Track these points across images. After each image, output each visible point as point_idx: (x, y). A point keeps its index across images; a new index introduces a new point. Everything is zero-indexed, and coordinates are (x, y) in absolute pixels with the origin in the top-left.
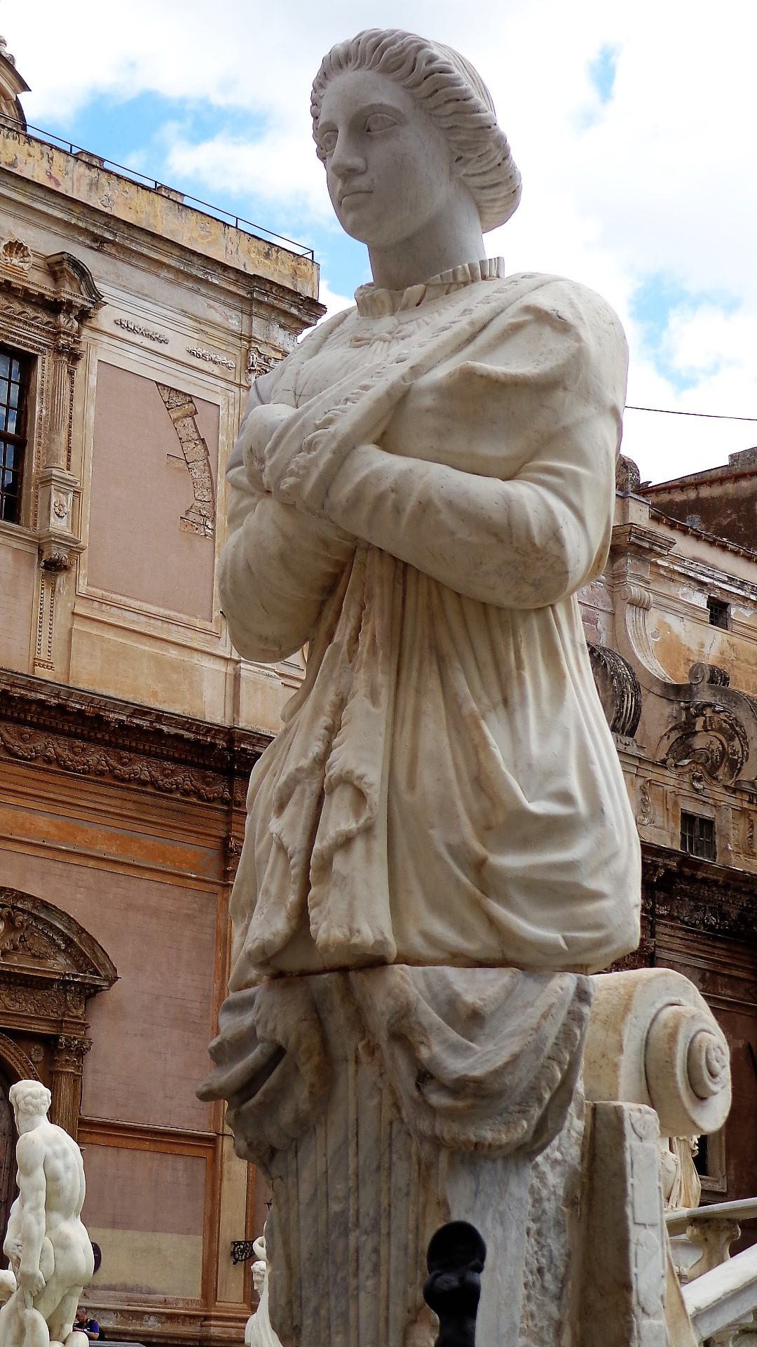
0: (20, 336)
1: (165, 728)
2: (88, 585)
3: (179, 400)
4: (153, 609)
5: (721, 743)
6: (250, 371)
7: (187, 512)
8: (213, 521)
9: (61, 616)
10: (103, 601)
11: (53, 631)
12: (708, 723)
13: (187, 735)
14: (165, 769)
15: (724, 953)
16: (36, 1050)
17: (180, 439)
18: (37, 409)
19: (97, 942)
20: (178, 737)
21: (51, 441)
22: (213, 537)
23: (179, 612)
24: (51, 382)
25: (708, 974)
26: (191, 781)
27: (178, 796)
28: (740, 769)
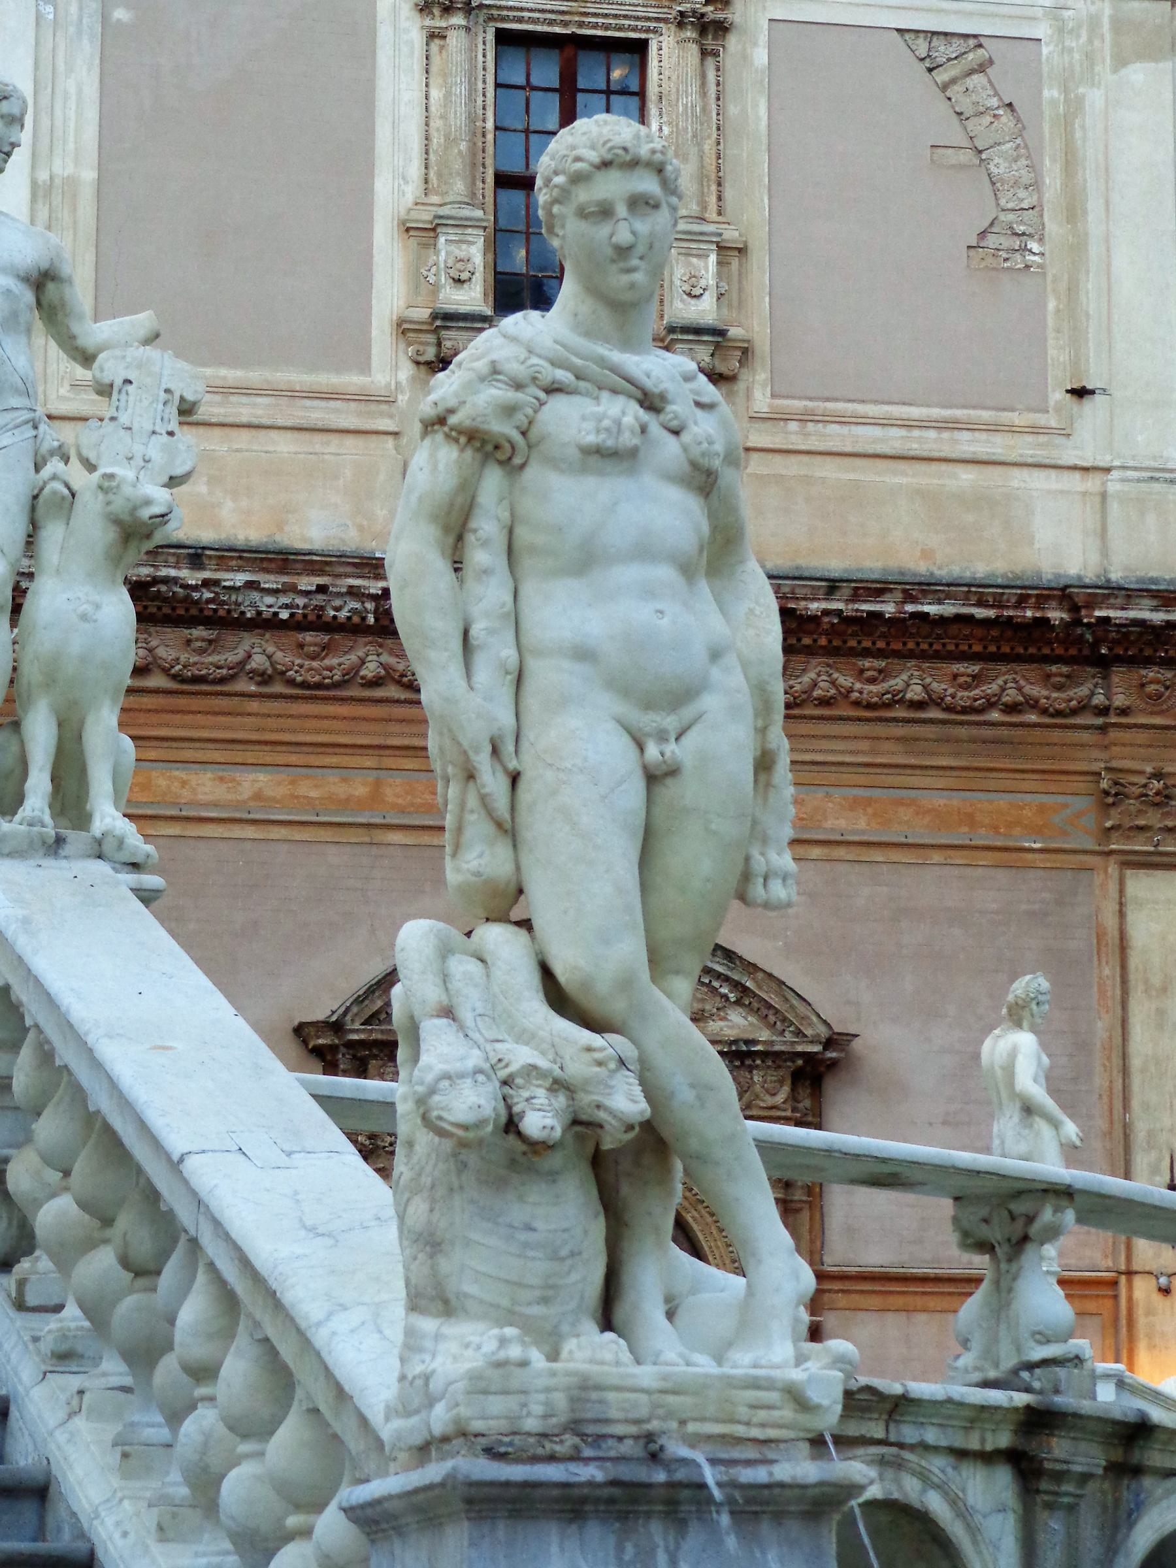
0: (606, 16)
1: (931, 609)
2: (773, 396)
3: (943, 50)
4: (915, 412)
7: (983, 234)
8: (1041, 240)
10: (805, 418)
13: (980, 613)
14: (955, 676)
17: (959, 114)
19: (784, 983)
20: (959, 618)
23: (974, 407)
26: (1020, 689)
27: (995, 715)
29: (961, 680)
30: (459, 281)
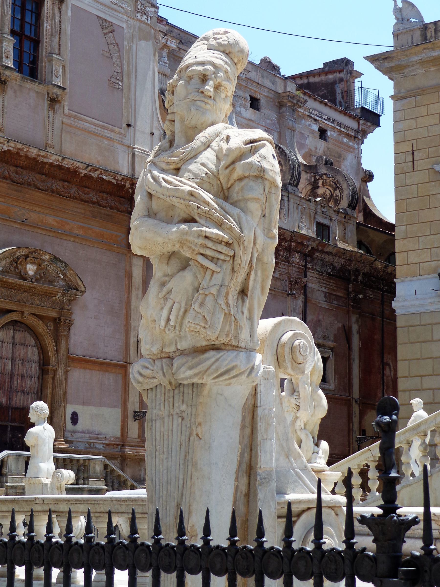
1: (104, 177)
4: (97, 122)
5: (331, 191)
6: (138, 12)
7: (111, 77)
8: (122, 82)
9: (57, 124)
11: (54, 131)
12: (324, 183)
13: (114, 181)
14: (102, 197)
15: (333, 285)
16: (50, 324)
18: (45, 25)
21: (52, 41)
22: (122, 90)
24: (51, 13)
25: (327, 294)
28: (339, 203)
29: (104, 198)
30: (7, 57)
